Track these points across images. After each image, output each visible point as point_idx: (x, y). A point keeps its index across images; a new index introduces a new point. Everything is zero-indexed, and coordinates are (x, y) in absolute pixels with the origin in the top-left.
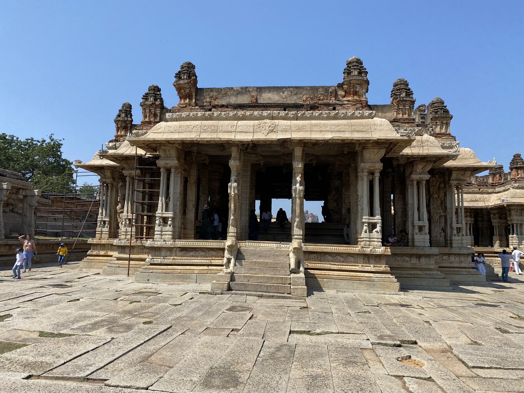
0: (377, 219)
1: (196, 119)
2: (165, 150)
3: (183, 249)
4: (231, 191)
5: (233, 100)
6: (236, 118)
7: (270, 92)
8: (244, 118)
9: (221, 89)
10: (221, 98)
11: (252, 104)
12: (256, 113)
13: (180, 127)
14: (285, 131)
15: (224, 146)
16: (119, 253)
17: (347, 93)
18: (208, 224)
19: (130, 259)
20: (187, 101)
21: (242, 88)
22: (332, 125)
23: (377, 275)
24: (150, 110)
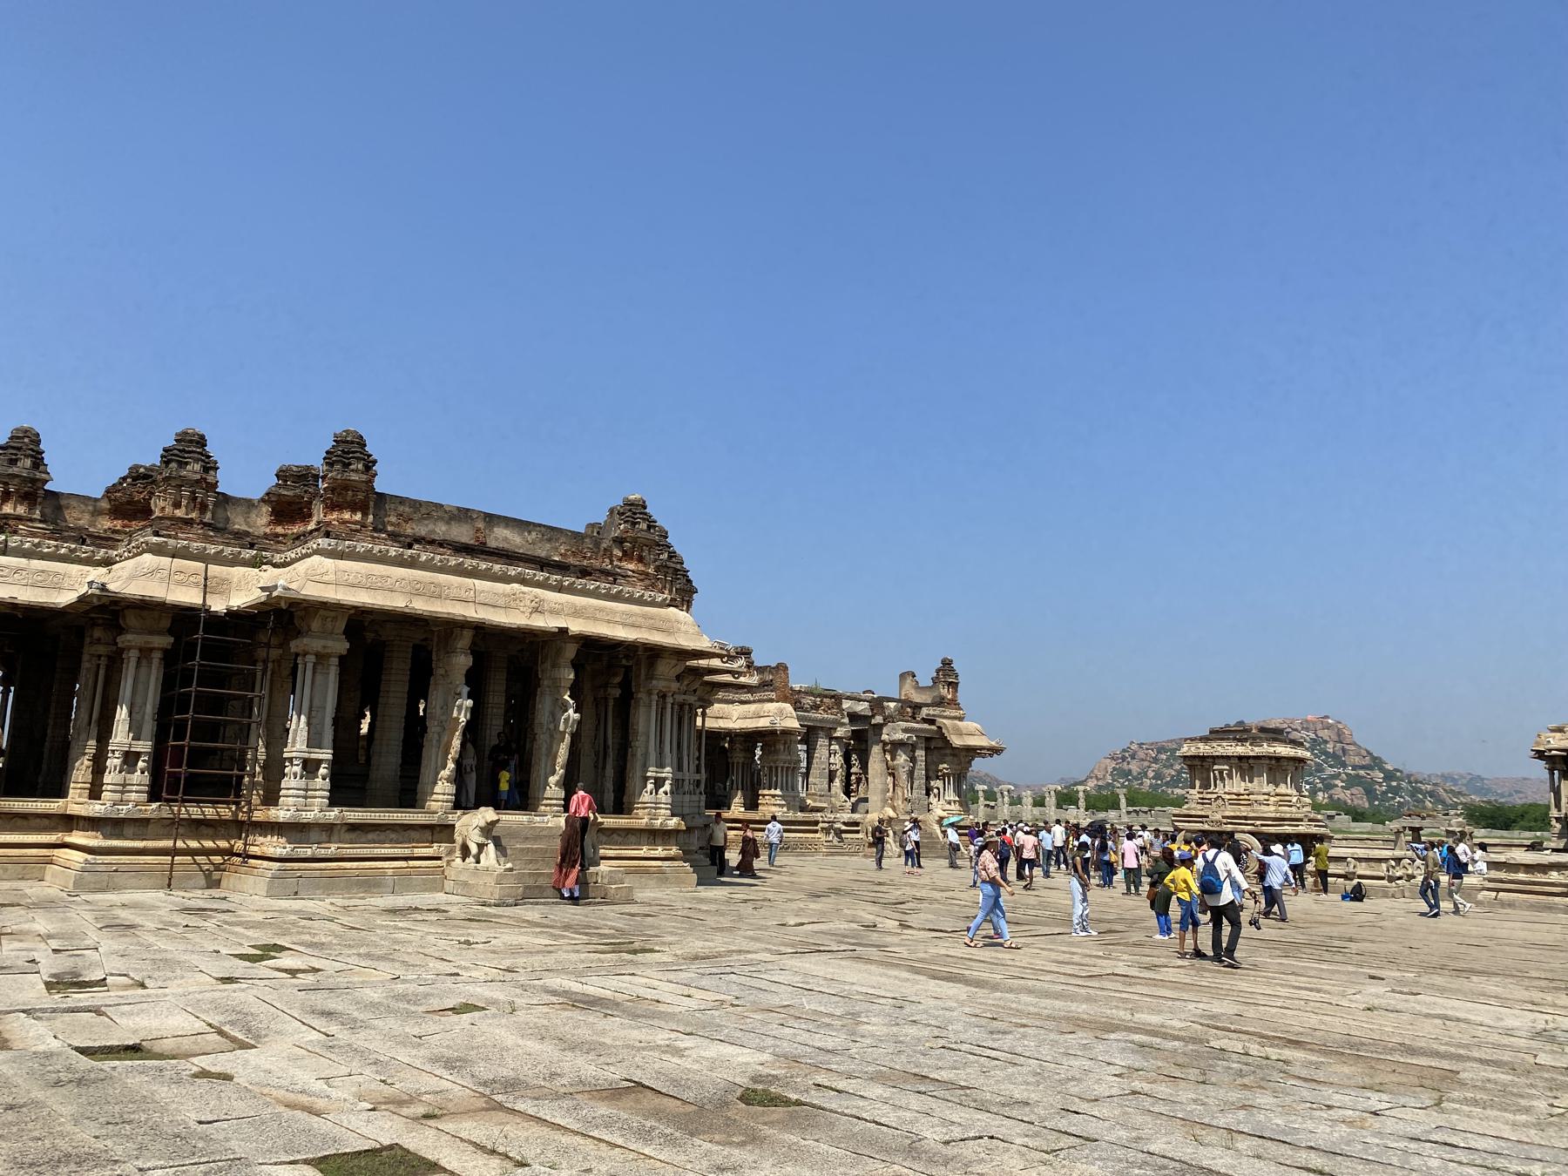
0: (667, 772)
1: (383, 559)
3: (354, 827)
5: (441, 530)
7: (507, 526)
8: (474, 574)
9: (420, 503)
10: (420, 520)
11: (478, 545)
12: (497, 567)
13: (368, 576)
14: (554, 612)
15: (450, 628)
16: (105, 837)
17: (627, 555)
19: (174, 852)
20: (358, 517)
24: (193, 493)
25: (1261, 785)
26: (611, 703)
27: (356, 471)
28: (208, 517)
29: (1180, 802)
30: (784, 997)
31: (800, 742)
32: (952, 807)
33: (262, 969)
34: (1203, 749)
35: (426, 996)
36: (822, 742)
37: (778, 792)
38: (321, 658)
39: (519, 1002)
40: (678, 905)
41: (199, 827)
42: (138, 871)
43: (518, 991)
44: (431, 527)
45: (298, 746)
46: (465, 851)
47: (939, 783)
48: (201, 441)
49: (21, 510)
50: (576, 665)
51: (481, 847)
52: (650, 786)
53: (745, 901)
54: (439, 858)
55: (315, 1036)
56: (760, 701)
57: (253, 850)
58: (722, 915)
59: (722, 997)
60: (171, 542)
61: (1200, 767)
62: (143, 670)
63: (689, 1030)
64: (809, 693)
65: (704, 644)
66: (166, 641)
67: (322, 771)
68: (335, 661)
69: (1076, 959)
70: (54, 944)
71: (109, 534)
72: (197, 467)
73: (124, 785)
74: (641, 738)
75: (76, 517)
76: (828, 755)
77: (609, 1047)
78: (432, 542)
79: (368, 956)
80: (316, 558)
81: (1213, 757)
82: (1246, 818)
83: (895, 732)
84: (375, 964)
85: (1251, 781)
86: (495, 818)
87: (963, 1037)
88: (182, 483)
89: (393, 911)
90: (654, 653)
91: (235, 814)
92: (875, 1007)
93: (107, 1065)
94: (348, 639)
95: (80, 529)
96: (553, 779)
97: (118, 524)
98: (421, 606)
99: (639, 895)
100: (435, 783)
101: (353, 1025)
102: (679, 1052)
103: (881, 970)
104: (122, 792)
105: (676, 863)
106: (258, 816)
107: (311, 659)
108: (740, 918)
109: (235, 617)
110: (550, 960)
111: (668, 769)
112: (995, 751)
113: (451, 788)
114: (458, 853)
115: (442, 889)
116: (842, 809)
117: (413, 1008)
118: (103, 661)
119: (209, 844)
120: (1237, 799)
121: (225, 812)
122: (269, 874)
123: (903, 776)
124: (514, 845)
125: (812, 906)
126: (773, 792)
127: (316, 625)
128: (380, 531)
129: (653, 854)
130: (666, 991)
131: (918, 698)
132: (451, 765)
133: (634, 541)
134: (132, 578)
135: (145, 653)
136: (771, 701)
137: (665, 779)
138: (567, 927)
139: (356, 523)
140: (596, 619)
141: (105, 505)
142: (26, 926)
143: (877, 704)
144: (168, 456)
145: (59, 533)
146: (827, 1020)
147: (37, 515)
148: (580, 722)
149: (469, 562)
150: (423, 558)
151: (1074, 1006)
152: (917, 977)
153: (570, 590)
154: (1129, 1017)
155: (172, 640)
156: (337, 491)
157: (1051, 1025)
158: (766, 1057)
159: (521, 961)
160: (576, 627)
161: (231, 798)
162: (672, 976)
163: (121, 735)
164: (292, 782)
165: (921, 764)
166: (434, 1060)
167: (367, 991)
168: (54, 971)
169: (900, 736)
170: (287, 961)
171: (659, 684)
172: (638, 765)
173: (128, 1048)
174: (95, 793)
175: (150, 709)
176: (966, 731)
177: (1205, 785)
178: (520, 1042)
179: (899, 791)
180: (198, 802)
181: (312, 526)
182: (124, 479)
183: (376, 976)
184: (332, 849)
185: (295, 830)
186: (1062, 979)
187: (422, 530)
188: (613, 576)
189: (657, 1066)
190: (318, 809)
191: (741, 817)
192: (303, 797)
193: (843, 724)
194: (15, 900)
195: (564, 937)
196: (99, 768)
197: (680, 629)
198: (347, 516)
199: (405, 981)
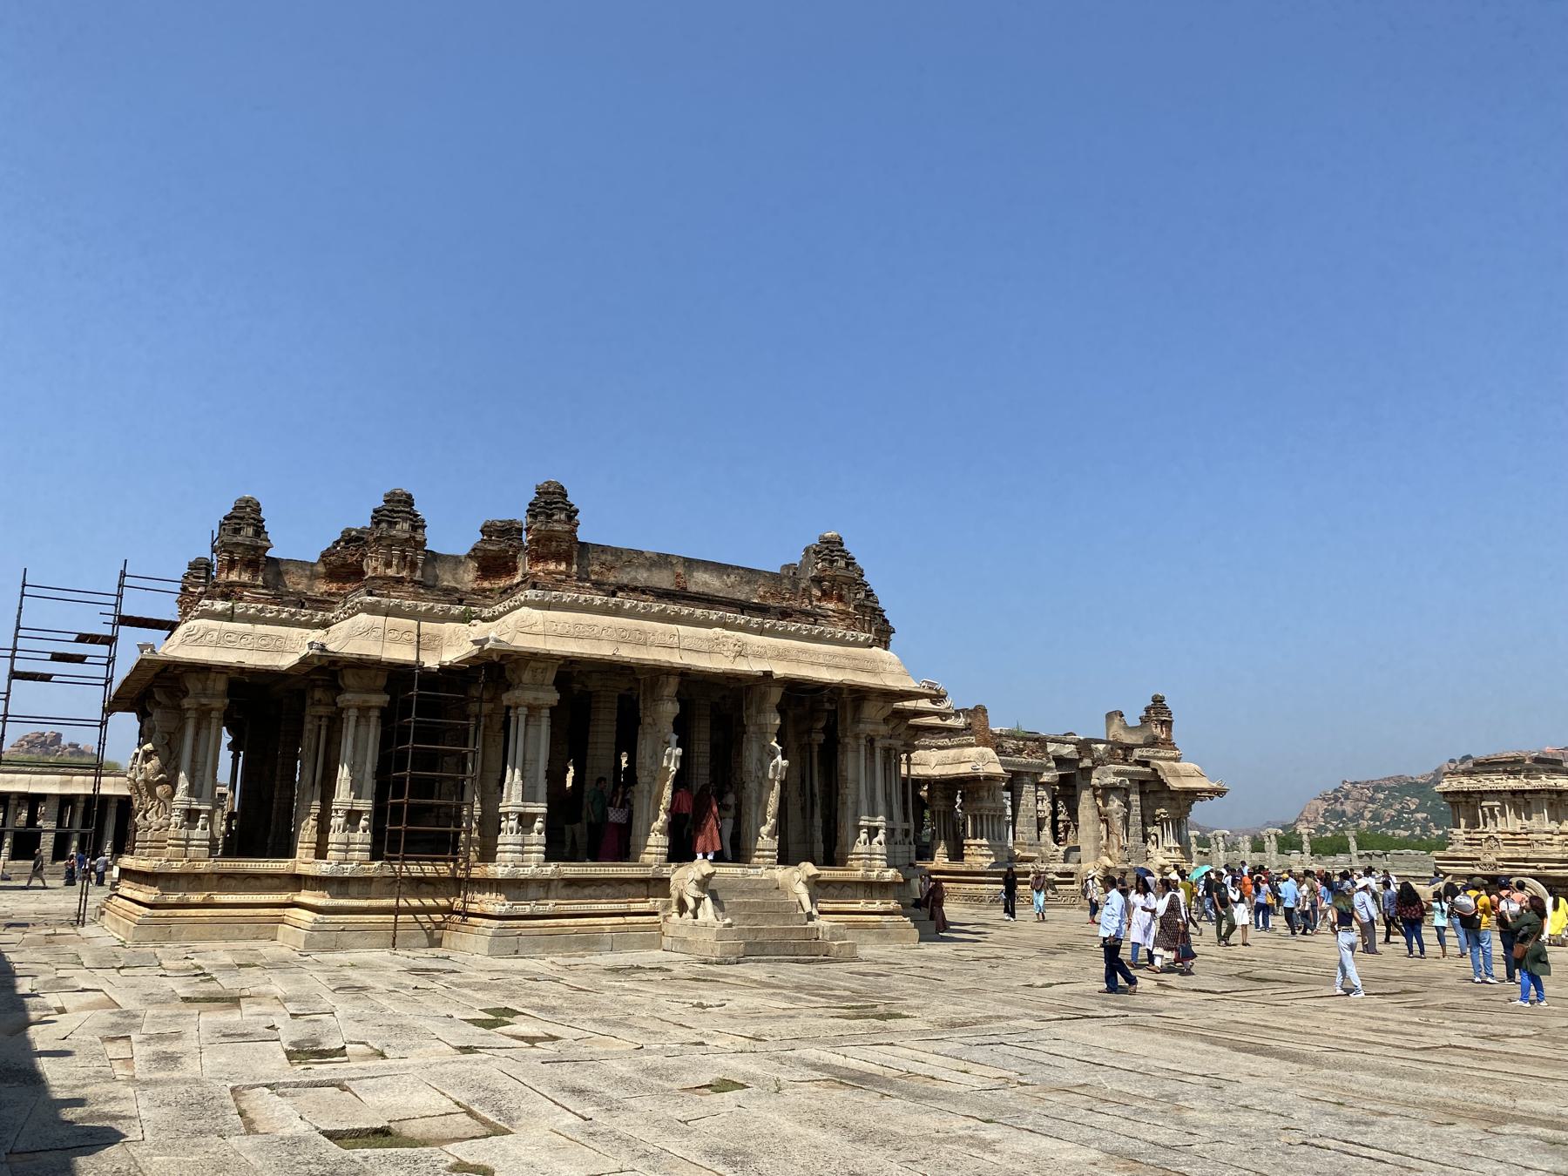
0: (880, 821)
1: (588, 608)
2: (534, 670)
5: (642, 577)
6: (663, 617)
8: (676, 619)
11: (678, 590)
12: (698, 612)
14: (759, 656)
17: (826, 595)
18: (587, 827)
19: (397, 911)
20: (563, 567)
22: (826, 654)
23: (887, 918)
24: (403, 551)
25: (1541, 823)
26: (816, 749)
27: (558, 521)
28: (418, 575)
29: (1443, 843)
30: (1073, 1075)
31: (1007, 789)
32: (1173, 854)
33: (497, 1036)
34: (1467, 783)
35: (678, 1069)
36: (1028, 788)
37: (984, 841)
38: (533, 710)
39: (784, 1077)
40: (907, 963)
41: (420, 885)
42: (363, 930)
43: (775, 1064)
44: (633, 574)
45: (513, 801)
47: (1157, 829)
48: (408, 500)
49: (245, 577)
50: (781, 710)
51: (698, 901)
52: (863, 836)
53: (978, 959)
54: (655, 914)
55: (570, 1119)
56: (958, 746)
57: (473, 908)
58: (959, 974)
59: (1005, 1073)
60: (384, 600)
61: (1465, 805)
62: (362, 729)
63: (987, 1116)
64: (1011, 736)
65: (910, 685)
66: (381, 699)
67: (538, 825)
68: (546, 712)
69: (1392, 1026)
70: (292, 1008)
71: (326, 597)
72: (406, 526)
73: (348, 844)
74: (851, 785)
75: (296, 582)
76: (1035, 802)
77: (906, 1138)
78: (635, 589)
79: (602, 1021)
80: (525, 609)
81: (1480, 792)
82: (1526, 860)
83: (1105, 776)
84: (615, 1031)
85: (1529, 818)
86: (711, 870)
87: (1321, 1129)
88: (393, 542)
89: (615, 970)
90: (860, 694)
91: (453, 871)
92: (1187, 1087)
93: (358, 1154)
94: (559, 689)
95: (299, 593)
96: (764, 830)
97: (334, 587)
98: (628, 653)
99: (865, 951)
101: (610, 1107)
102: (986, 1146)
103: (1169, 1040)
104: (346, 851)
105: (896, 918)
106: (476, 872)
107: (523, 711)
108: (981, 978)
109: (448, 673)
110: (796, 1026)
111: (881, 818)
112: (1220, 793)
114: (674, 908)
115: (660, 946)
116: (1053, 859)
117: (668, 1085)
118: (324, 722)
119: (429, 902)
120: (1513, 839)
121: (444, 870)
122: (489, 932)
123: (1117, 823)
124: (731, 900)
125: (1053, 964)
126: (978, 841)
127: (526, 677)
128: (585, 580)
129: (871, 908)
130: (932, 1062)
131: (1128, 739)
132: (663, 816)
133: (833, 579)
134: (349, 637)
135: (364, 711)
136: (971, 745)
137: (877, 829)
138: (799, 988)
139: (561, 573)
140: (799, 661)
141: (321, 569)
142: (263, 989)
143: (1085, 746)
144: (378, 517)
145: (279, 598)
146: (1141, 1104)
147: (260, 581)
148: (788, 769)
149: (672, 608)
150: (627, 606)
151: (1431, 1088)
152: (1220, 1049)
153: (772, 633)
154: (1509, 1103)
156: (542, 543)
157: (1420, 1113)
158: (1093, 1154)
159: (765, 1028)
160: (780, 670)
161: (449, 855)
162: (937, 1047)
163: (343, 795)
164: (508, 837)
165: (1136, 810)
166: (710, 1153)
167: (614, 1063)
168: (294, 1038)
169: (1111, 780)
170: (522, 1027)
171: (866, 728)
172: (850, 813)
173: (376, 1132)
174: (321, 852)
175: (369, 768)
176: (1183, 773)
177: (1473, 824)
178: (801, 1130)
179: (1114, 839)
180: (418, 859)
181: (518, 579)
182: (338, 542)
183: (616, 1046)
184: (550, 906)
185: (512, 887)
186: (1393, 1052)
187: (624, 578)
188: (814, 617)
189: (971, 1164)
190: (534, 866)
191: (946, 868)
192: (519, 853)
193: (1050, 769)
194: (252, 961)
195: (800, 999)
196: (323, 829)
197: (885, 668)
198: (552, 566)
199: (650, 1052)
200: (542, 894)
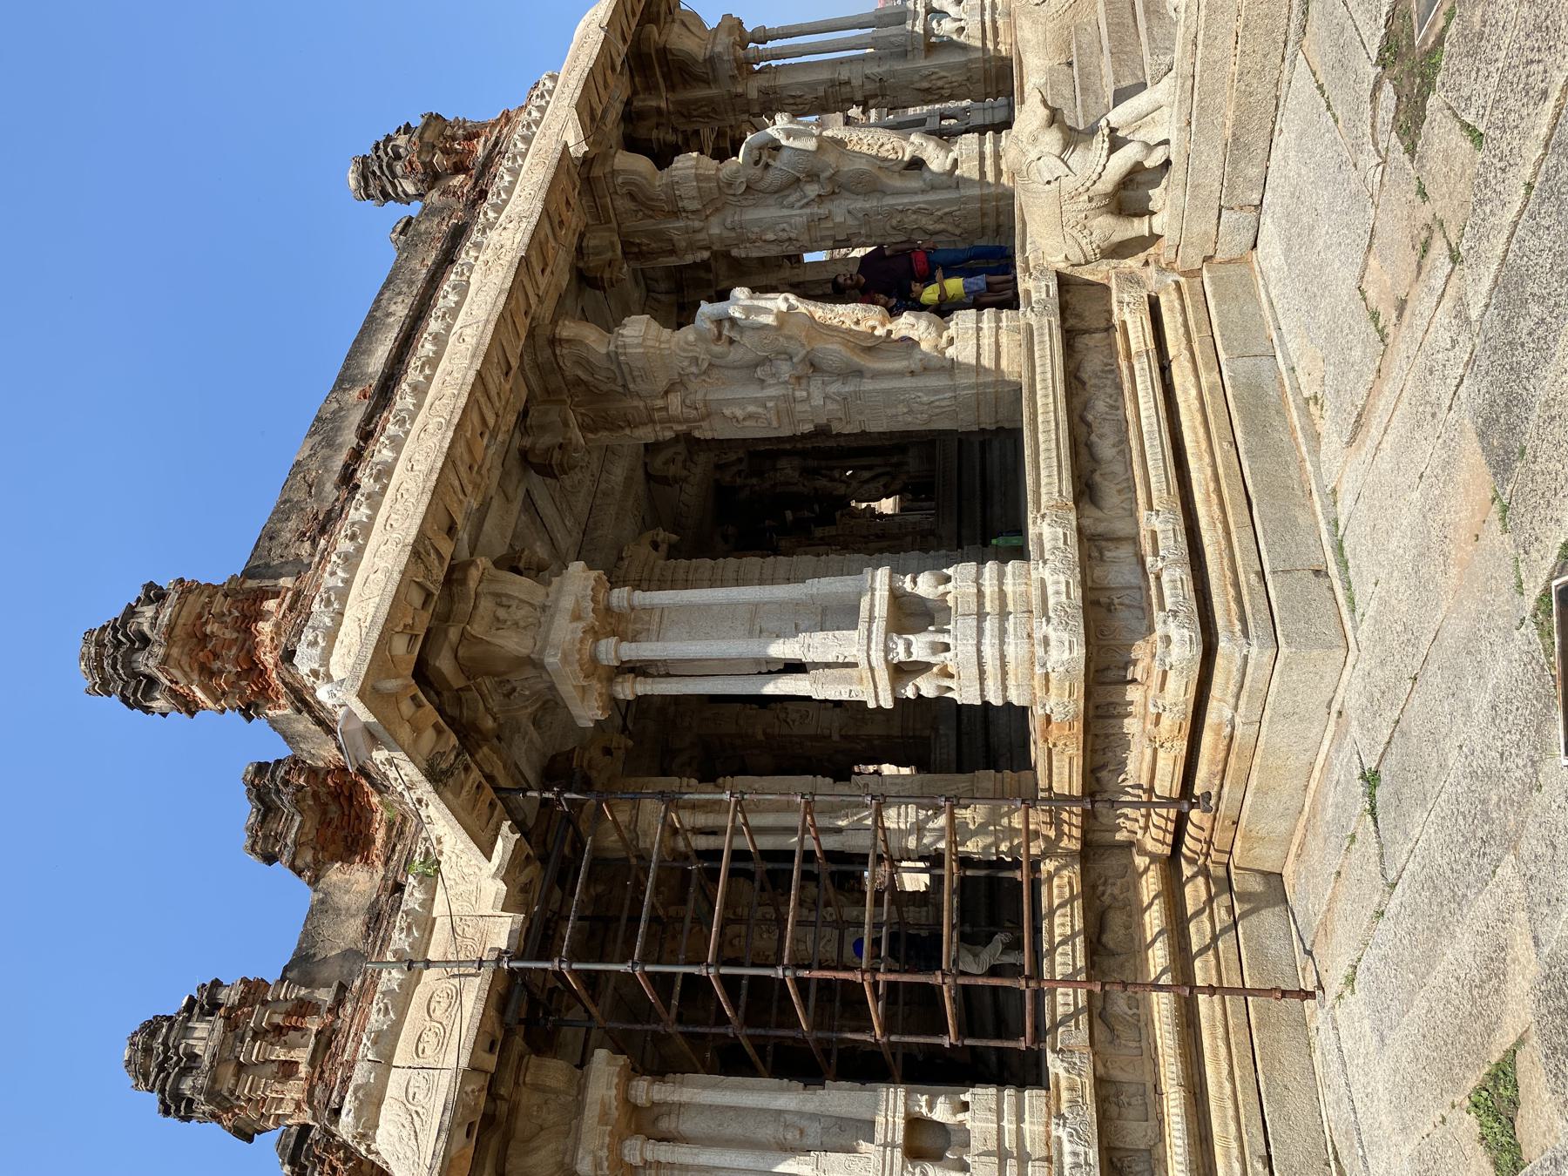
3: (1085, 490)
4: (767, 311)
21: (311, 434)
28: (325, 996)
41: (1106, 947)
46: (1128, 196)
57: (1167, 782)
62: (687, 1126)
66: (605, 1069)
67: (924, 586)
72: (201, 1028)
73: (1002, 1155)
96: (937, 160)
100: (952, 367)
113: (964, 320)
121: (1061, 885)
127: (512, 643)
132: (908, 325)
155: (601, 1055)
161: (1022, 875)
164: (964, 670)
175: (787, 1098)
180: (1036, 931)
184: (1157, 524)
192: (1002, 633)
200: (1125, 551)
